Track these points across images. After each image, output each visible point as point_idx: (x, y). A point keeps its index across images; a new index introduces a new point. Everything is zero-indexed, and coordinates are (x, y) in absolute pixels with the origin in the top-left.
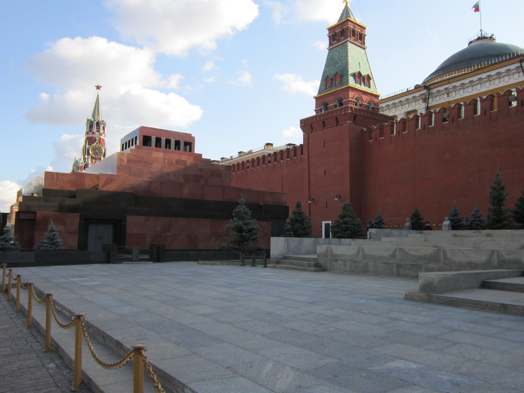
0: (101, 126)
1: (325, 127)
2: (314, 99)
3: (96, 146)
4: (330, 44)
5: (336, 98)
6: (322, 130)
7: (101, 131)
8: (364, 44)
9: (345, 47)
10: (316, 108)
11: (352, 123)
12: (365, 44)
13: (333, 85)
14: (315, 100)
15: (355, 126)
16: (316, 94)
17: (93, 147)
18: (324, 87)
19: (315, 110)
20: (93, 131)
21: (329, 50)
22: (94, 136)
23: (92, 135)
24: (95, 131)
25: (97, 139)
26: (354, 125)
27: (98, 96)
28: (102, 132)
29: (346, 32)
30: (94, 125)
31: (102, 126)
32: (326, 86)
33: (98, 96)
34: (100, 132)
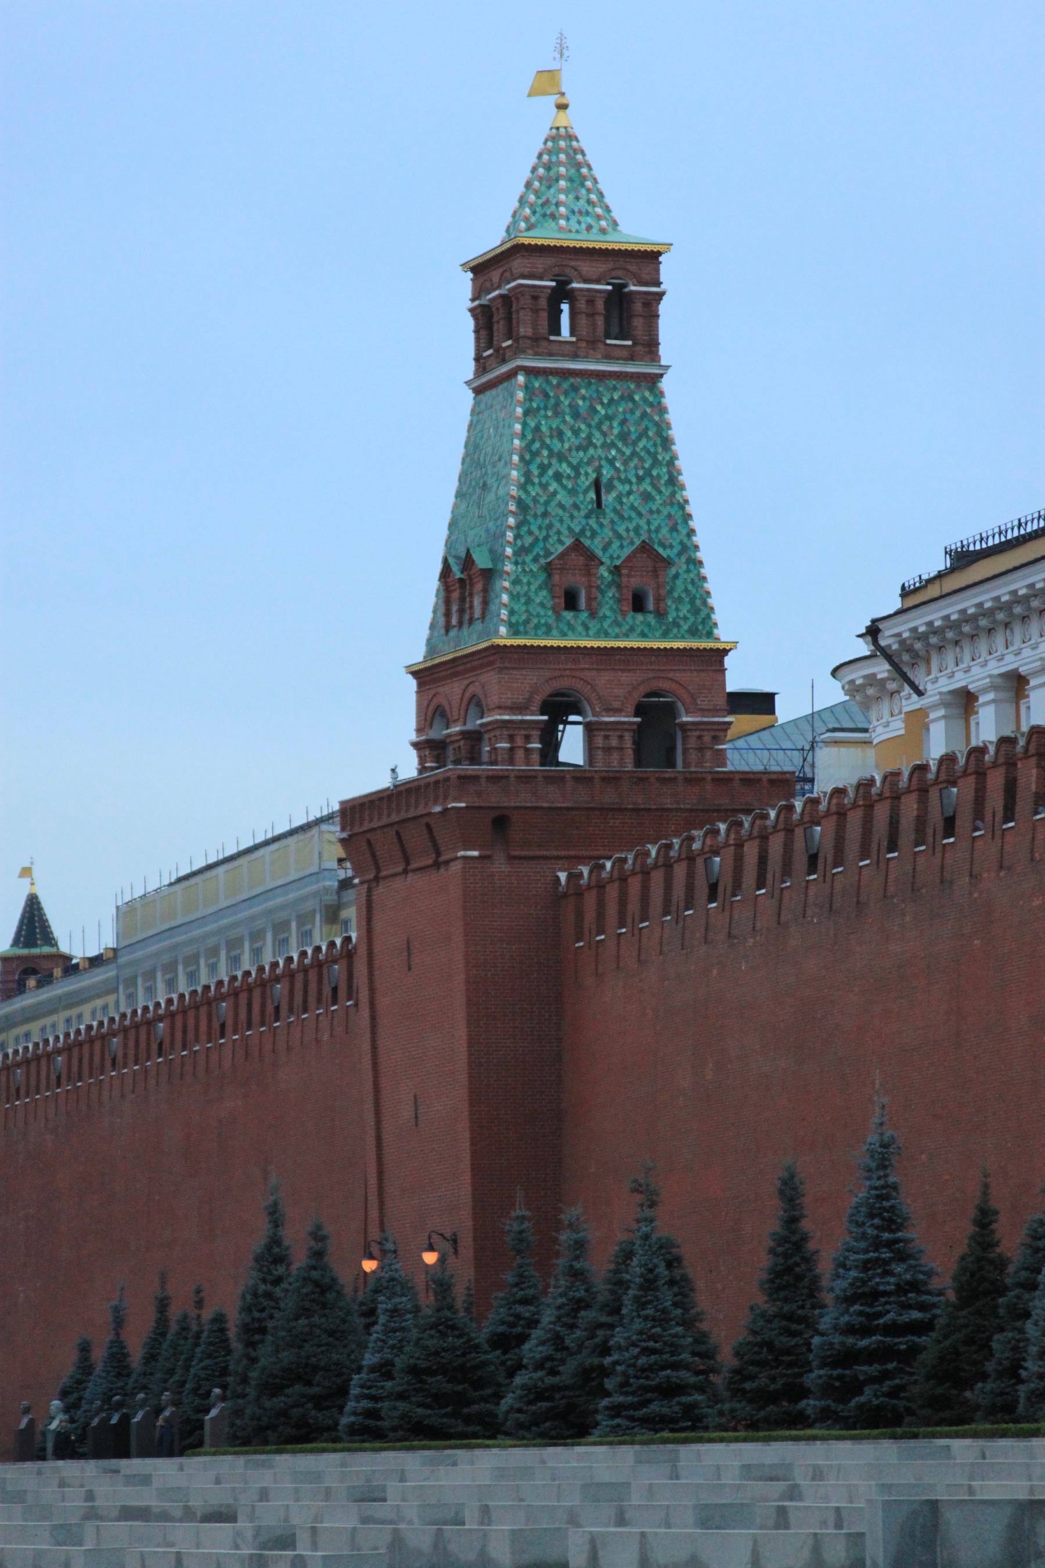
1: (413, 866)
2: (410, 676)
4: (481, 363)
5: (468, 695)
6: (400, 874)
8: (650, 347)
9: (512, 397)
10: (419, 730)
11: (480, 857)
12: (662, 350)
13: (467, 617)
14: (412, 683)
15: (505, 868)
16: (417, 655)
18: (442, 620)
19: (416, 745)
21: (478, 391)
26: (500, 866)
29: (518, 312)
32: (448, 614)
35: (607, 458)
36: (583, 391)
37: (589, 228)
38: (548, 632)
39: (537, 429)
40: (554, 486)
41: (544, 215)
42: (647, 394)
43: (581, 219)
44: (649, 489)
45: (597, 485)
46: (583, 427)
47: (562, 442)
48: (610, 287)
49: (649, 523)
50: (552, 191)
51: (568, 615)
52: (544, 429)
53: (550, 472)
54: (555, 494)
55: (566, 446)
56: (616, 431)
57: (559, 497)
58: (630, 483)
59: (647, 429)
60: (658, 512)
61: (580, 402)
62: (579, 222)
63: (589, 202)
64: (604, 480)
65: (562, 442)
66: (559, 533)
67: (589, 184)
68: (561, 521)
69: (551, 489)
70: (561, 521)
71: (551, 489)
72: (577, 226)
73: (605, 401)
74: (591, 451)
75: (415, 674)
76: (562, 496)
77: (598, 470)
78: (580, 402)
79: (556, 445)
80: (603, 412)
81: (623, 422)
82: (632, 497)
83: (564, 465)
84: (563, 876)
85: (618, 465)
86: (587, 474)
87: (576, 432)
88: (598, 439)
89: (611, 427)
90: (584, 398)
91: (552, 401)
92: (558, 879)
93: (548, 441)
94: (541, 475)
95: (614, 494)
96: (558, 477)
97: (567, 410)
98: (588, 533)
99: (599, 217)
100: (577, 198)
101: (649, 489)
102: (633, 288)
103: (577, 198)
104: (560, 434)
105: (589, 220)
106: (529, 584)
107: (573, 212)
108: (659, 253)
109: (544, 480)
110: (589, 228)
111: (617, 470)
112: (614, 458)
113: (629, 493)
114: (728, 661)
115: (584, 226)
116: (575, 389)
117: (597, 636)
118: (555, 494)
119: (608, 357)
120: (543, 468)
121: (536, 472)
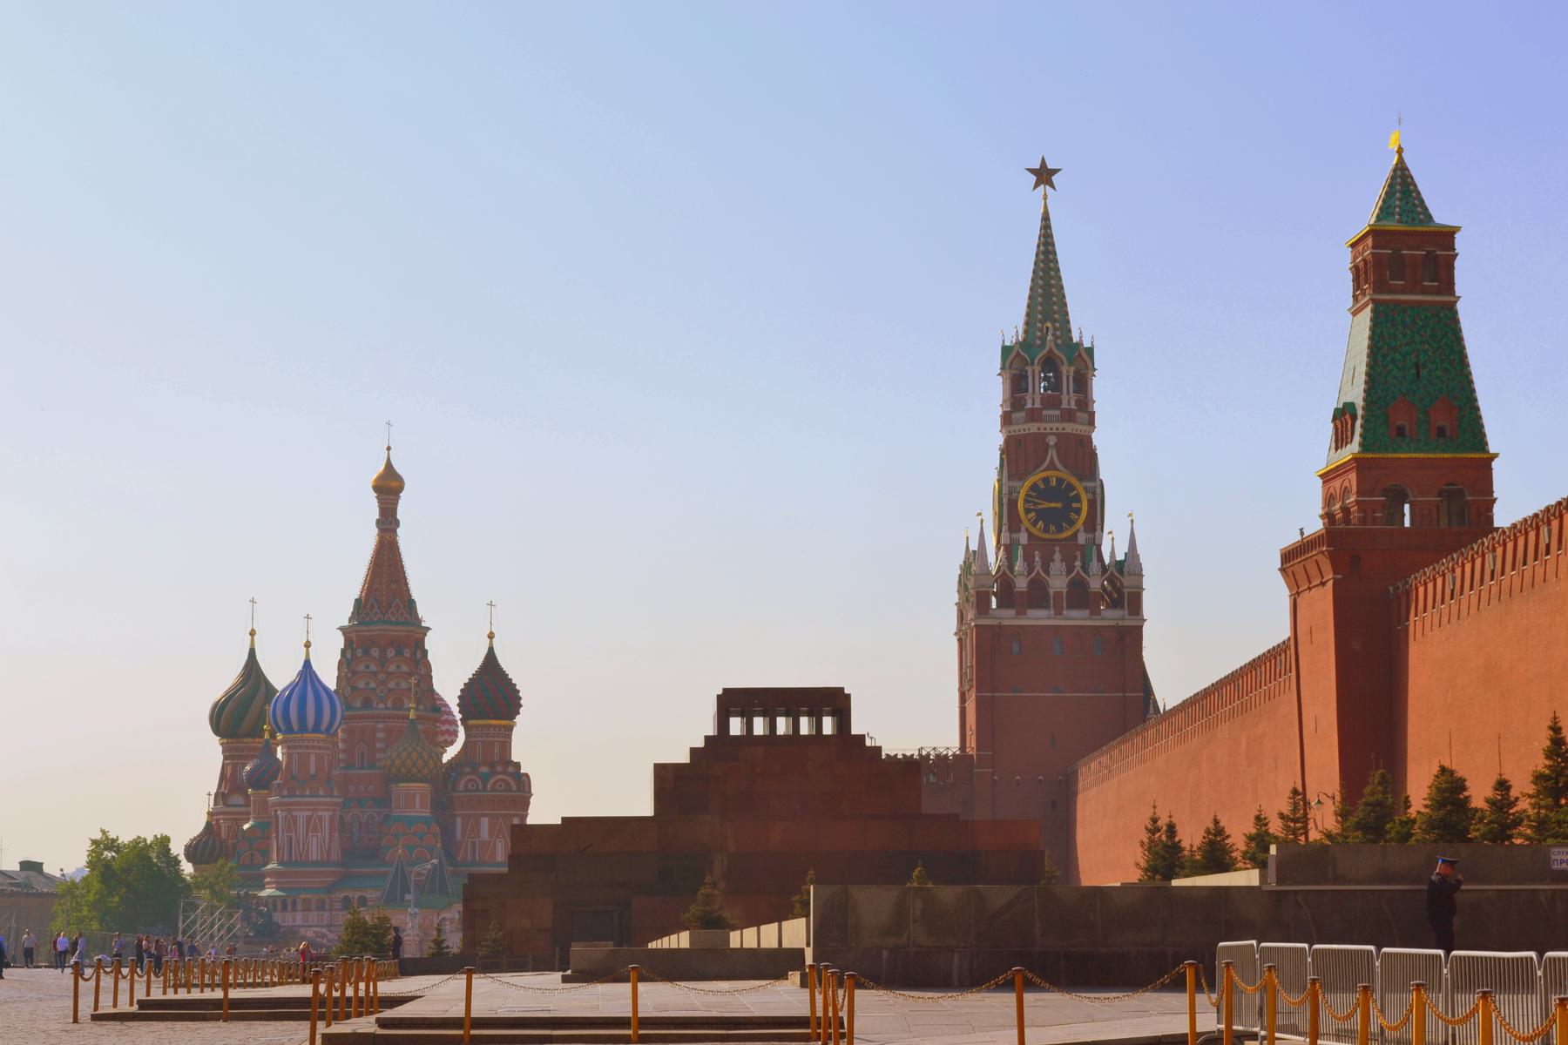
0: (1064, 373)
3: (1046, 480)
7: (1068, 400)
14: (1320, 481)
17: (1034, 487)
20: (1029, 405)
22: (1033, 428)
23: (1027, 426)
24: (1037, 405)
25: (1052, 440)
27: (1046, 218)
28: (1073, 406)
30: (1029, 373)
31: (1067, 371)
33: (1046, 218)
34: (1065, 405)
35: (1423, 350)
36: (1409, 312)
37: (1413, 219)
38: (1386, 451)
39: (1381, 334)
40: (1391, 367)
41: (1388, 214)
42: (1447, 312)
43: (1410, 215)
44: (1448, 367)
45: (1417, 366)
46: (1409, 332)
47: (1396, 341)
48: (1424, 253)
49: (1447, 387)
50: (1393, 200)
51: (1398, 440)
52: (1385, 334)
53: (1389, 359)
54: (1392, 370)
55: (1399, 343)
56: (1428, 335)
57: (1393, 372)
58: (1437, 363)
59: (1447, 333)
60: (1453, 380)
61: (1407, 319)
62: (1407, 216)
63: (1414, 205)
64: (1420, 363)
65: (1396, 341)
66: (1393, 393)
67: (1414, 195)
68: (1395, 386)
69: (1389, 368)
70: (1395, 386)
71: (1389, 368)
72: (1406, 218)
73: (1422, 317)
74: (1413, 346)
75: (1321, 476)
76: (1395, 372)
77: (1417, 356)
78: (1407, 319)
79: (1393, 343)
80: (1421, 323)
81: (1433, 330)
82: (1438, 372)
83: (1397, 355)
84: (1391, 588)
85: (1430, 353)
86: (1410, 359)
87: (1405, 336)
88: (1418, 338)
89: (1426, 332)
90: (1409, 316)
91: (1390, 318)
92: (1389, 590)
93: (1388, 341)
94: (1383, 360)
95: (1426, 370)
96: (1393, 361)
97: (1400, 323)
98: (1411, 393)
99: (1419, 213)
100: (1407, 203)
101: (1448, 367)
102: (1438, 253)
103: (1407, 203)
104: (1395, 338)
105: (1414, 215)
106: (1375, 422)
107: (1404, 211)
108: (1454, 233)
109: (1385, 363)
110: (1413, 219)
111: (1429, 356)
112: (1427, 350)
113: (1437, 368)
114: (1494, 464)
115: (1410, 218)
116: (1405, 311)
117: (1415, 452)
118: (1392, 370)
119: (1426, 291)
120: (1384, 356)
121: (1380, 359)
